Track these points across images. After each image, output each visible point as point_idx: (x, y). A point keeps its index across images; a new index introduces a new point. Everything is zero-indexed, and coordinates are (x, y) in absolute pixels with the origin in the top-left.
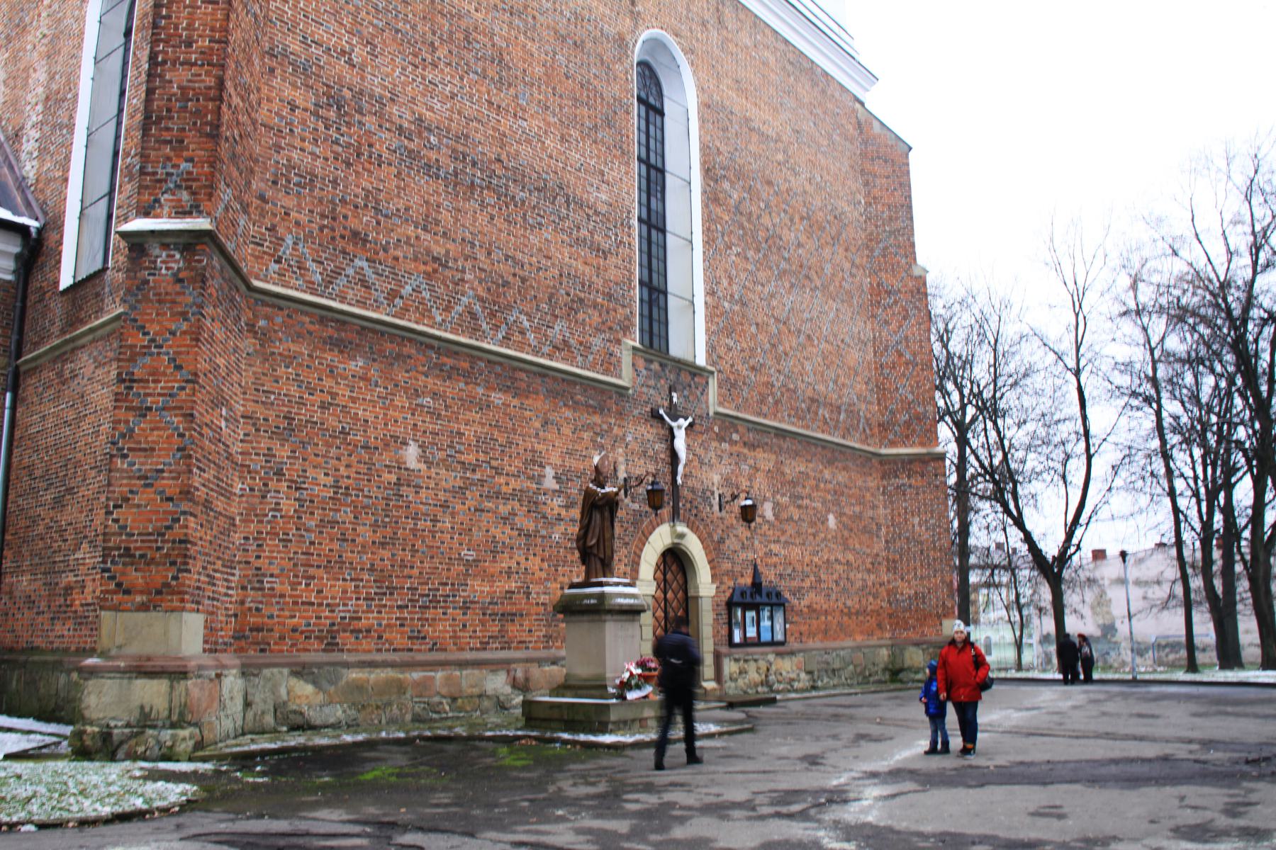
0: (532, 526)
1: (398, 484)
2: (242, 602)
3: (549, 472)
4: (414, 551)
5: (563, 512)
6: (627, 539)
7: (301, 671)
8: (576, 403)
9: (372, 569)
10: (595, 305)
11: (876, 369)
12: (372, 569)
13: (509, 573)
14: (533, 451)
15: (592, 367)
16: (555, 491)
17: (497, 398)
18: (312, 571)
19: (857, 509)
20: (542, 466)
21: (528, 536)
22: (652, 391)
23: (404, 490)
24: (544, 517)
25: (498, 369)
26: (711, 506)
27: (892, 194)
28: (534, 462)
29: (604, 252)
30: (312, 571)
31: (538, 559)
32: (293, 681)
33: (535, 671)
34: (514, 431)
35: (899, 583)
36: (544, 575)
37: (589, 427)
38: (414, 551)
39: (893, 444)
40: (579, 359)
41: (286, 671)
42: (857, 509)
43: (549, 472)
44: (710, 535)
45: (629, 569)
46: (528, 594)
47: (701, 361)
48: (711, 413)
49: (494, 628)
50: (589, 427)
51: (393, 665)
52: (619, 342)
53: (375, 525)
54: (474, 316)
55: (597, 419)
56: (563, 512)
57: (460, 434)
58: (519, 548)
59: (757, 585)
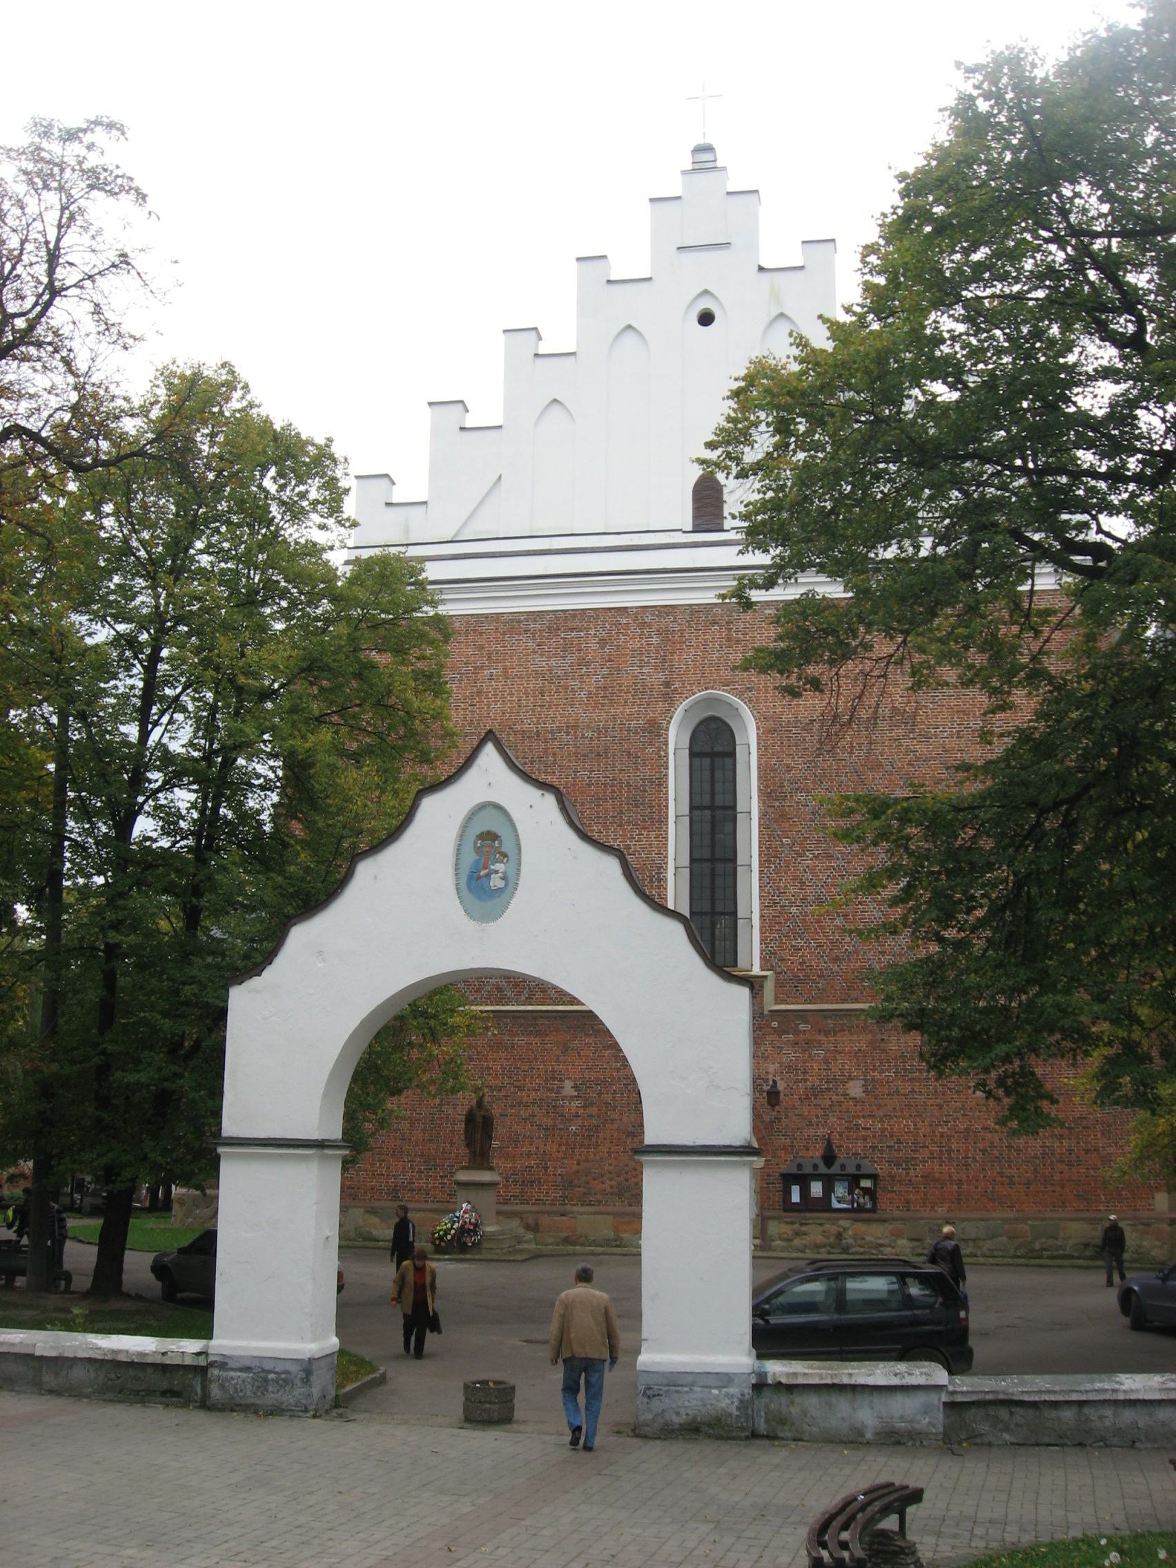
0: (550, 1122)
1: (441, 1105)
3: (568, 1084)
4: (452, 1143)
7: (372, 1211)
9: (422, 1155)
12: (422, 1155)
13: (529, 1154)
14: (554, 1071)
16: (572, 1097)
17: (520, 1040)
18: (383, 1157)
20: (561, 1080)
21: (547, 1129)
23: (445, 1108)
25: (522, 1021)
28: (553, 1079)
30: (383, 1157)
32: (367, 1216)
33: (545, 1220)
34: (536, 1059)
38: (452, 1143)
43: (568, 1084)
46: (546, 1168)
47: (756, 970)
48: (766, 1012)
49: (516, 1190)
51: (431, 1210)
53: (424, 1130)
54: (500, 989)
57: (488, 1068)
58: (539, 1138)
59: (829, 1158)
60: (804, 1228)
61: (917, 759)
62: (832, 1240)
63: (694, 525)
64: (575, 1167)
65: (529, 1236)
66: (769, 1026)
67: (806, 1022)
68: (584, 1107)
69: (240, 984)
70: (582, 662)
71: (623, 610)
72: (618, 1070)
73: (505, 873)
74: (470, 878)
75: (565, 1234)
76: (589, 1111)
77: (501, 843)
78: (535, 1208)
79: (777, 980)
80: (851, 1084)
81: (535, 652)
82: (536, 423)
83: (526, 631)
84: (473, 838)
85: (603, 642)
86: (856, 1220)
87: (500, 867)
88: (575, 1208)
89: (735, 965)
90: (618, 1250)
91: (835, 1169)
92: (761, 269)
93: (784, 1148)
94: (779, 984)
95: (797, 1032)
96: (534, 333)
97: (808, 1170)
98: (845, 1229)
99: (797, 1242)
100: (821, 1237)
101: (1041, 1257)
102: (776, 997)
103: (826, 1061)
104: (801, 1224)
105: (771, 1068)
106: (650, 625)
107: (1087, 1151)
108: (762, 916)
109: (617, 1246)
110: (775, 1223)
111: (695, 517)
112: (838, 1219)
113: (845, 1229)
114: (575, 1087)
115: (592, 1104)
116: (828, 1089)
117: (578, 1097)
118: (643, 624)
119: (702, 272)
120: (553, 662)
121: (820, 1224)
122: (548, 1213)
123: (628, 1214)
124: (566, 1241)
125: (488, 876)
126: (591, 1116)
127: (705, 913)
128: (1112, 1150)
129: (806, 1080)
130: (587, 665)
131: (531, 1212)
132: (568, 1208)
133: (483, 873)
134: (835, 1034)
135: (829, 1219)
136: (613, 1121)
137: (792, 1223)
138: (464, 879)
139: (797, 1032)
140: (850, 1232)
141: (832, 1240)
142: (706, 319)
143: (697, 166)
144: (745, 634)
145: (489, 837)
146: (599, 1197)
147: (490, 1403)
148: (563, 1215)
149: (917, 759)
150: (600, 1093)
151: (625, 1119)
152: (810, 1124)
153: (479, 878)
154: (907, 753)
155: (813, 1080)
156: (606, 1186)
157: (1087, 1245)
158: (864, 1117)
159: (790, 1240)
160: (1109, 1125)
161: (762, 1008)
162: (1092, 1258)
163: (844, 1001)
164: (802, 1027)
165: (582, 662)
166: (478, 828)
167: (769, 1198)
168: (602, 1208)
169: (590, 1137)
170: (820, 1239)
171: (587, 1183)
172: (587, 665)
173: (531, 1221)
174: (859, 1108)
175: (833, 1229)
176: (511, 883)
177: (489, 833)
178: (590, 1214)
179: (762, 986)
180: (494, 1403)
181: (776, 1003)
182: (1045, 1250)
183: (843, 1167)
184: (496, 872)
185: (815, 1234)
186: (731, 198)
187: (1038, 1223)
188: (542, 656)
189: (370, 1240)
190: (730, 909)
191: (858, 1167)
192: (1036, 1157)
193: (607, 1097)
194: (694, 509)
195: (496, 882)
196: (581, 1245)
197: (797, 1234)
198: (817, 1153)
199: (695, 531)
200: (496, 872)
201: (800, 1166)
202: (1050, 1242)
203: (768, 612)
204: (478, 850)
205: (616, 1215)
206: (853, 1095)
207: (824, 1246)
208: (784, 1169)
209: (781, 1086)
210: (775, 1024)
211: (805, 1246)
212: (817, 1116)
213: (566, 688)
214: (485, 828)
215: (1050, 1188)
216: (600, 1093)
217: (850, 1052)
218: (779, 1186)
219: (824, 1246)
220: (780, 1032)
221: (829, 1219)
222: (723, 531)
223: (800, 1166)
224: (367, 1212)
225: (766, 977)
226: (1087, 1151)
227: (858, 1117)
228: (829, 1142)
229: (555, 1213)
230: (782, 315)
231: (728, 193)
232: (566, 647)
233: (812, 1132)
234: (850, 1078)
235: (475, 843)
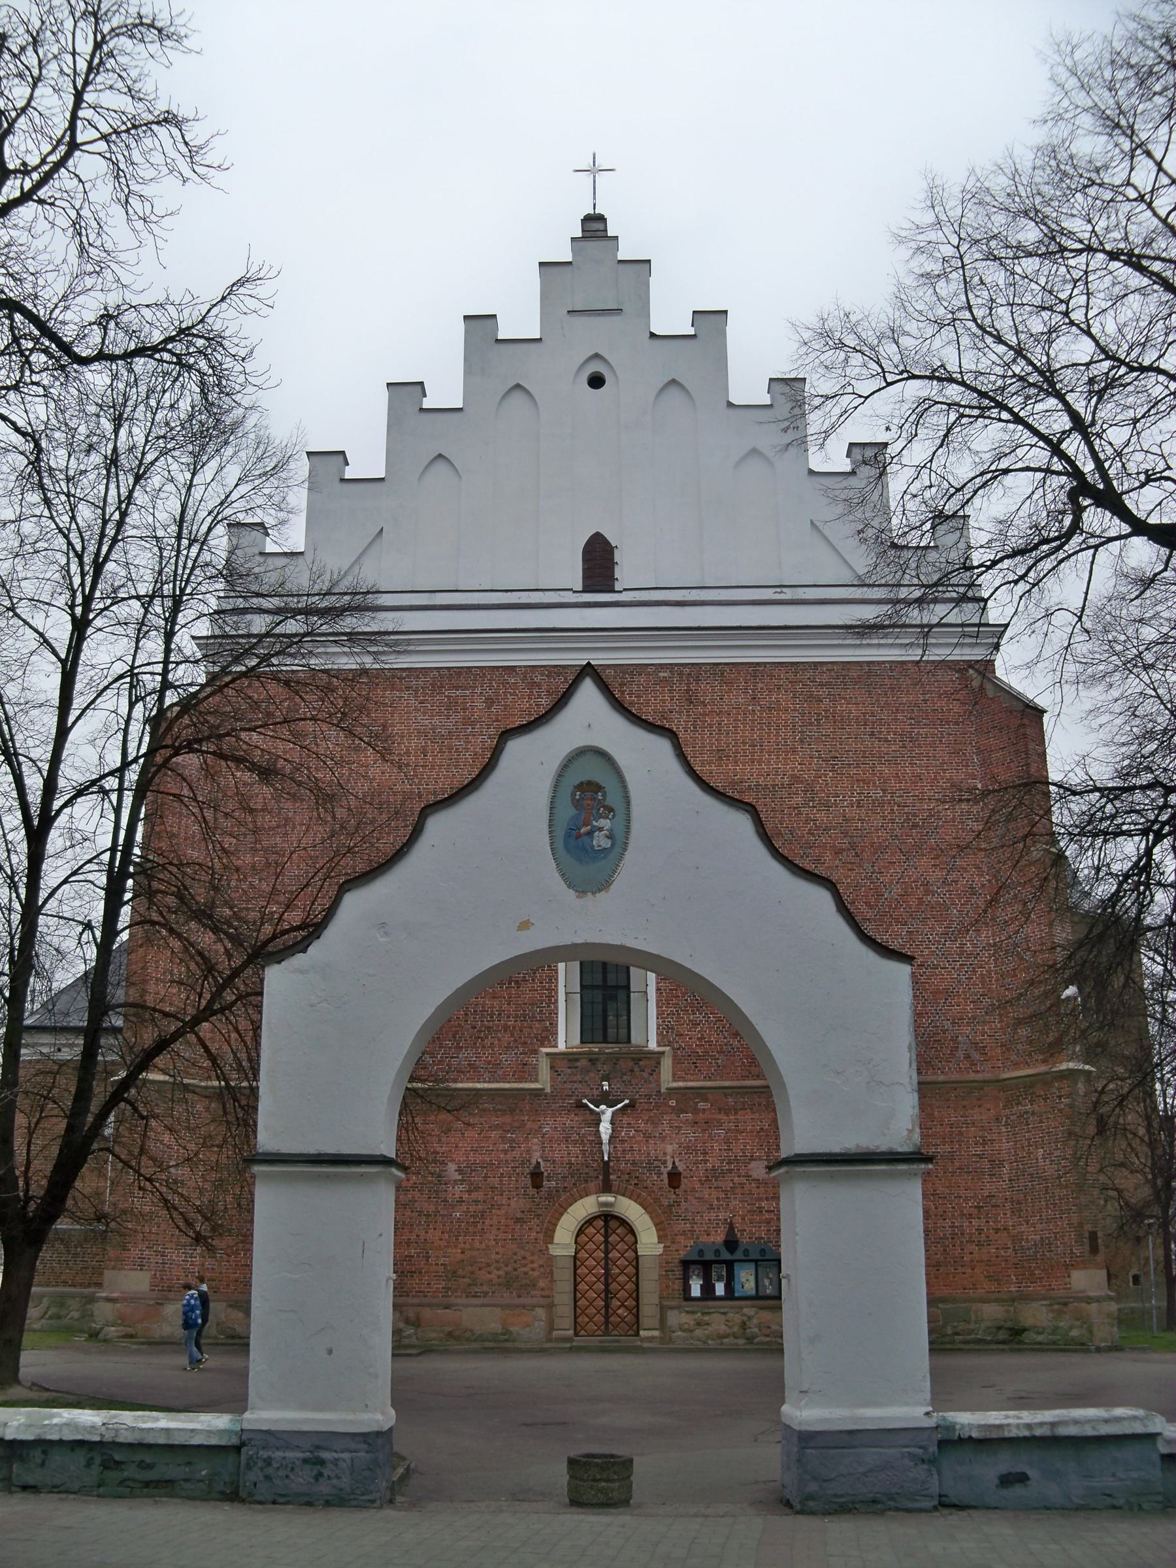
0: (432, 1208)
2: (203, 1265)
3: (452, 1167)
5: (465, 1196)
6: (539, 1212)
8: (484, 1110)
10: (506, 1028)
11: (997, 980)
15: (503, 1079)
19: (947, 1148)
20: (443, 1163)
22: (580, 1086)
24: (445, 1201)
26: (660, 1174)
27: (1009, 768)
29: (517, 982)
31: (438, 1233)
32: (230, 1310)
33: (427, 1313)
35: (1024, 1228)
36: (443, 1243)
37: (497, 1127)
39: (1016, 1065)
40: (486, 1076)
41: (225, 1304)
42: (947, 1148)
43: (452, 1167)
44: (657, 1200)
45: (541, 1236)
46: (427, 1258)
47: (653, 1045)
50: (497, 1127)
52: (535, 1052)
55: (508, 1119)
56: (465, 1196)
59: (731, 1244)
60: (706, 1318)
61: (818, 828)
62: (736, 1329)
63: (584, 586)
64: (460, 1257)
65: (411, 1331)
66: (667, 1105)
67: (706, 1100)
68: (469, 1192)
69: (279, 962)
70: (468, 721)
71: (511, 669)
72: (505, 1152)
73: (611, 830)
74: (568, 836)
75: (448, 1329)
76: (474, 1195)
77: (604, 795)
78: (416, 1301)
79: (675, 1057)
80: (753, 1164)
81: (416, 710)
82: (420, 478)
83: (408, 688)
84: (570, 789)
85: (490, 702)
86: (762, 1308)
87: (603, 823)
88: (459, 1301)
89: (629, 1041)
90: (509, 1345)
91: (739, 1255)
92: (653, 335)
93: (684, 1233)
94: (676, 1061)
95: (696, 1111)
96: (419, 388)
97: (709, 1256)
98: (750, 1318)
99: (699, 1332)
100: (723, 1327)
101: (953, 1342)
102: (674, 1075)
103: (728, 1142)
104: (703, 1314)
105: (669, 1149)
106: (539, 686)
107: (997, 1231)
108: (658, 989)
109: (506, 1340)
110: (676, 1312)
111: (585, 578)
112: (741, 1308)
113: (750, 1318)
114: (459, 1171)
115: (477, 1189)
116: (730, 1171)
117: (463, 1180)
118: (533, 685)
119: (591, 336)
120: (436, 721)
121: (725, 1314)
122: (430, 1305)
123: (518, 1306)
124: (450, 1335)
125: (590, 834)
126: (476, 1202)
127: (597, 987)
128: (1024, 1228)
129: (706, 1161)
130: (473, 724)
131: (412, 1305)
132: (453, 1300)
133: (583, 830)
134: (736, 1113)
135: (732, 1307)
136: (500, 1206)
137: (693, 1313)
138: (560, 834)
139: (696, 1111)
140: (755, 1321)
141: (736, 1329)
142: (596, 381)
143: (588, 234)
144: (638, 697)
145: (590, 788)
146: (485, 1288)
147: (608, 1481)
148: (446, 1308)
149: (818, 828)
150: (486, 1177)
151: (513, 1203)
152: (711, 1207)
153: (579, 836)
154: (807, 822)
155: (713, 1161)
156: (493, 1276)
157: (999, 1328)
158: (767, 1199)
159: (691, 1331)
160: (1019, 1203)
161: (659, 1085)
162: (1003, 1342)
163: (744, 1078)
164: (701, 1105)
165: (468, 721)
166: (577, 775)
167: (667, 1286)
168: (485, 1301)
169: (475, 1224)
170: (723, 1328)
171: (472, 1273)
172: (473, 724)
173: (411, 1314)
174: (762, 1190)
175: (738, 1318)
176: (620, 842)
177: (589, 783)
178: (477, 1306)
179: (659, 1063)
180: (613, 1481)
181: (674, 1081)
182: (957, 1334)
183: (746, 1252)
184: (600, 829)
185: (718, 1322)
186: (621, 266)
187: (950, 1306)
188: (424, 713)
189: (233, 1337)
190: (623, 983)
191: (763, 1251)
192: (944, 1237)
193: (495, 1181)
194: (584, 570)
195: (600, 841)
196: (468, 1340)
197: (698, 1324)
198: (719, 1237)
199: (586, 589)
200: (600, 829)
201: (701, 1252)
202: (962, 1326)
203: (661, 674)
204: (577, 804)
205: (503, 1307)
206: (755, 1175)
207: (727, 1336)
208: (682, 1254)
209: (681, 1167)
210: (673, 1103)
211: (708, 1337)
212: (718, 1199)
213: (450, 748)
214: (585, 778)
215: (960, 1270)
216: (486, 1177)
217: (751, 1131)
218: (678, 1273)
219: (727, 1336)
220: (679, 1110)
221: (732, 1307)
222: (613, 591)
223: (701, 1252)
224: (231, 1306)
225: (663, 1053)
226: (997, 1231)
227: (761, 1199)
228: (731, 1224)
229: (438, 1306)
230: (673, 382)
231: (620, 262)
232: (452, 704)
233: (713, 1215)
234: (752, 1159)
235: (573, 795)
